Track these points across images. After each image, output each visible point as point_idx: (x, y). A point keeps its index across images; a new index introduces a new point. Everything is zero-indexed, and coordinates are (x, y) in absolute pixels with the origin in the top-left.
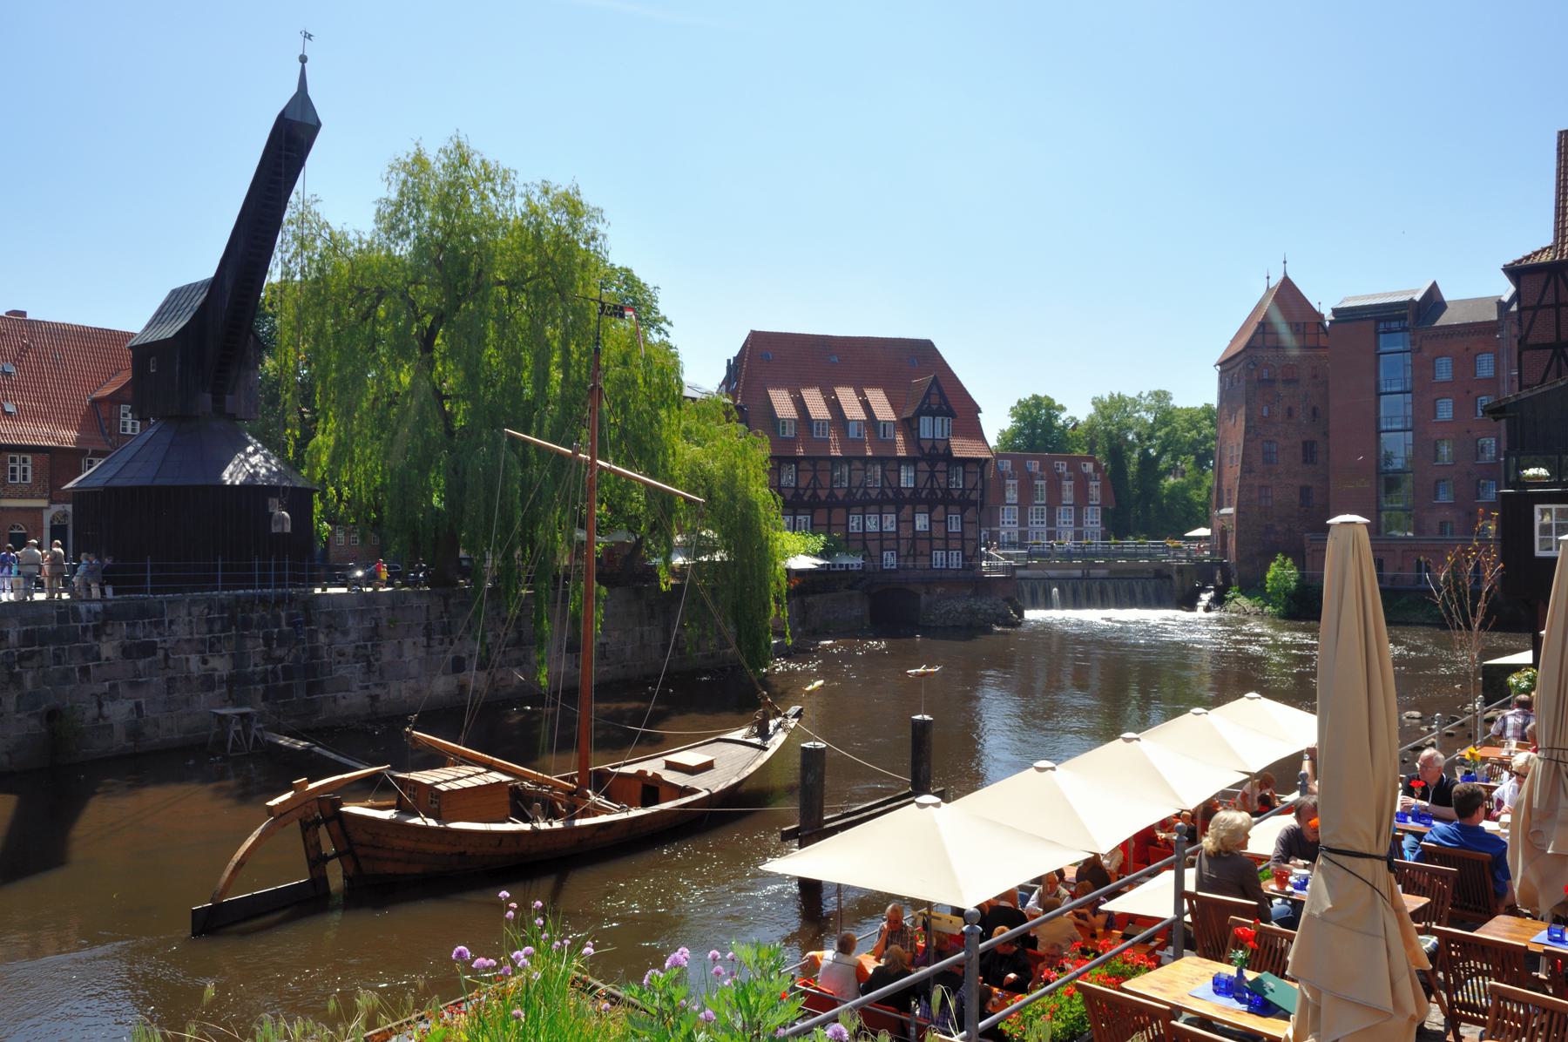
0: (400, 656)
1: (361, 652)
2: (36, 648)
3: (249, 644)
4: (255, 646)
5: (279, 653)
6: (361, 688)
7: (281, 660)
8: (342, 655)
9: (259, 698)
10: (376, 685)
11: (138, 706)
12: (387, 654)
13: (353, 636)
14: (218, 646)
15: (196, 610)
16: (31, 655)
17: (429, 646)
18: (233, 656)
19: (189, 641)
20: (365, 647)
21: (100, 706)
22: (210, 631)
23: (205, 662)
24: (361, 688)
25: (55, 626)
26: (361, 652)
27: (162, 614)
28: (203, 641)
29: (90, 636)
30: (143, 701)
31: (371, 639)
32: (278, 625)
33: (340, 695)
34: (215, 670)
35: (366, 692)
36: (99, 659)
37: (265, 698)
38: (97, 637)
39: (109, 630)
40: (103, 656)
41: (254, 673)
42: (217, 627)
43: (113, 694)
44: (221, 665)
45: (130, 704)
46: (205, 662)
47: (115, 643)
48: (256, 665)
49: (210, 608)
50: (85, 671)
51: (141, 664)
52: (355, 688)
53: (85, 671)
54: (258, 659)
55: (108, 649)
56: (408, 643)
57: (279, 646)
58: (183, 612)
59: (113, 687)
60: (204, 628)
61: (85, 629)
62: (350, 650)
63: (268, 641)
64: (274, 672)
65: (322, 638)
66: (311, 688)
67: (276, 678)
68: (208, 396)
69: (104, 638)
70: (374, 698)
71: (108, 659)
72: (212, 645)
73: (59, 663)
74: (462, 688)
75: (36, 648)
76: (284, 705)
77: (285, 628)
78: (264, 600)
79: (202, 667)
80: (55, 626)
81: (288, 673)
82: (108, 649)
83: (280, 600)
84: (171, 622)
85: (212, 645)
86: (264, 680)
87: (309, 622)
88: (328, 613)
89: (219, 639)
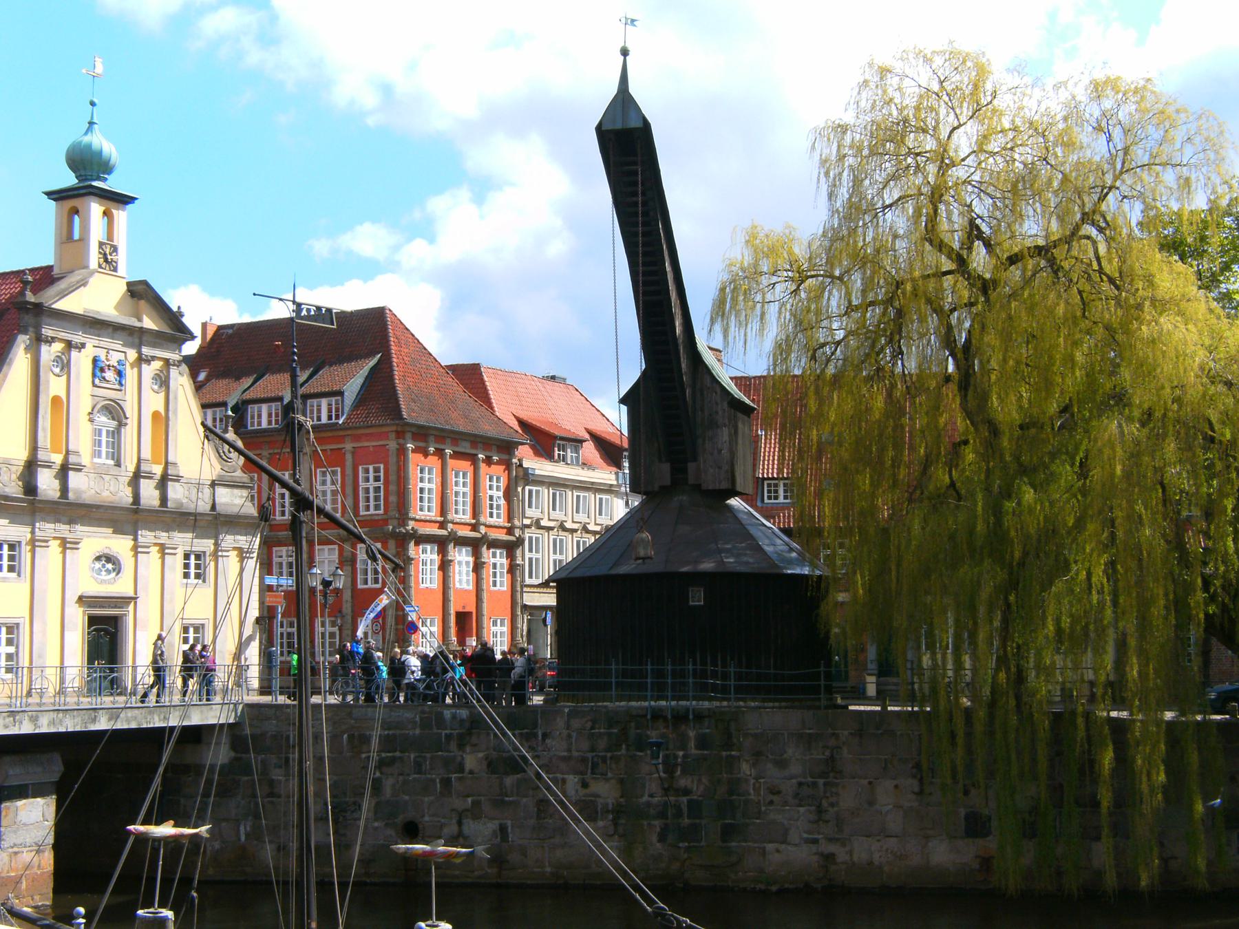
2: (398, 754)
4: (651, 773)
5: (683, 782)
6: (807, 841)
7: (686, 792)
8: (775, 791)
9: (654, 838)
10: (831, 840)
11: (503, 829)
12: (848, 797)
13: (795, 769)
15: (576, 723)
16: (393, 761)
17: (921, 792)
18: (621, 781)
19: (564, 759)
20: (815, 784)
21: (460, 823)
22: (593, 750)
24: (807, 841)
25: (417, 731)
27: (535, 726)
28: (584, 760)
29: (453, 746)
30: (509, 823)
31: (823, 775)
32: (683, 747)
33: (770, 847)
34: (599, 796)
35: (814, 848)
36: (461, 768)
37: (662, 838)
38: (461, 746)
39: (474, 740)
41: (648, 804)
42: (602, 744)
43: (475, 812)
44: (606, 791)
45: (493, 826)
46: (585, 785)
47: (481, 755)
48: (651, 793)
49: (594, 722)
50: (446, 782)
51: (509, 781)
52: (794, 836)
53: (446, 782)
54: (653, 786)
55: (471, 761)
57: (684, 772)
58: (560, 723)
59: (476, 804)
60: (585, 745)
61: (449, 737)
64: (678, 807)
65: (745, 768)
66: (728, 832)
67: (679, 814)
68: (666, 467)
69: (468, 749)
70: (829, 858)
71: (471, 772)
72: (594, 766)
73: (419, 772)
74: (986, 863)
75: (398, 754)
76: (688, 849)
77: (694, 751)
78: (657, 715)
79: (582, 792)
80: (417, 731)
81: (695, 808)
83: (680, 718)
84: (545, 736)
85: (594, 766)
86: (662, 815)
87: (728, 746)
89: (604, 760)
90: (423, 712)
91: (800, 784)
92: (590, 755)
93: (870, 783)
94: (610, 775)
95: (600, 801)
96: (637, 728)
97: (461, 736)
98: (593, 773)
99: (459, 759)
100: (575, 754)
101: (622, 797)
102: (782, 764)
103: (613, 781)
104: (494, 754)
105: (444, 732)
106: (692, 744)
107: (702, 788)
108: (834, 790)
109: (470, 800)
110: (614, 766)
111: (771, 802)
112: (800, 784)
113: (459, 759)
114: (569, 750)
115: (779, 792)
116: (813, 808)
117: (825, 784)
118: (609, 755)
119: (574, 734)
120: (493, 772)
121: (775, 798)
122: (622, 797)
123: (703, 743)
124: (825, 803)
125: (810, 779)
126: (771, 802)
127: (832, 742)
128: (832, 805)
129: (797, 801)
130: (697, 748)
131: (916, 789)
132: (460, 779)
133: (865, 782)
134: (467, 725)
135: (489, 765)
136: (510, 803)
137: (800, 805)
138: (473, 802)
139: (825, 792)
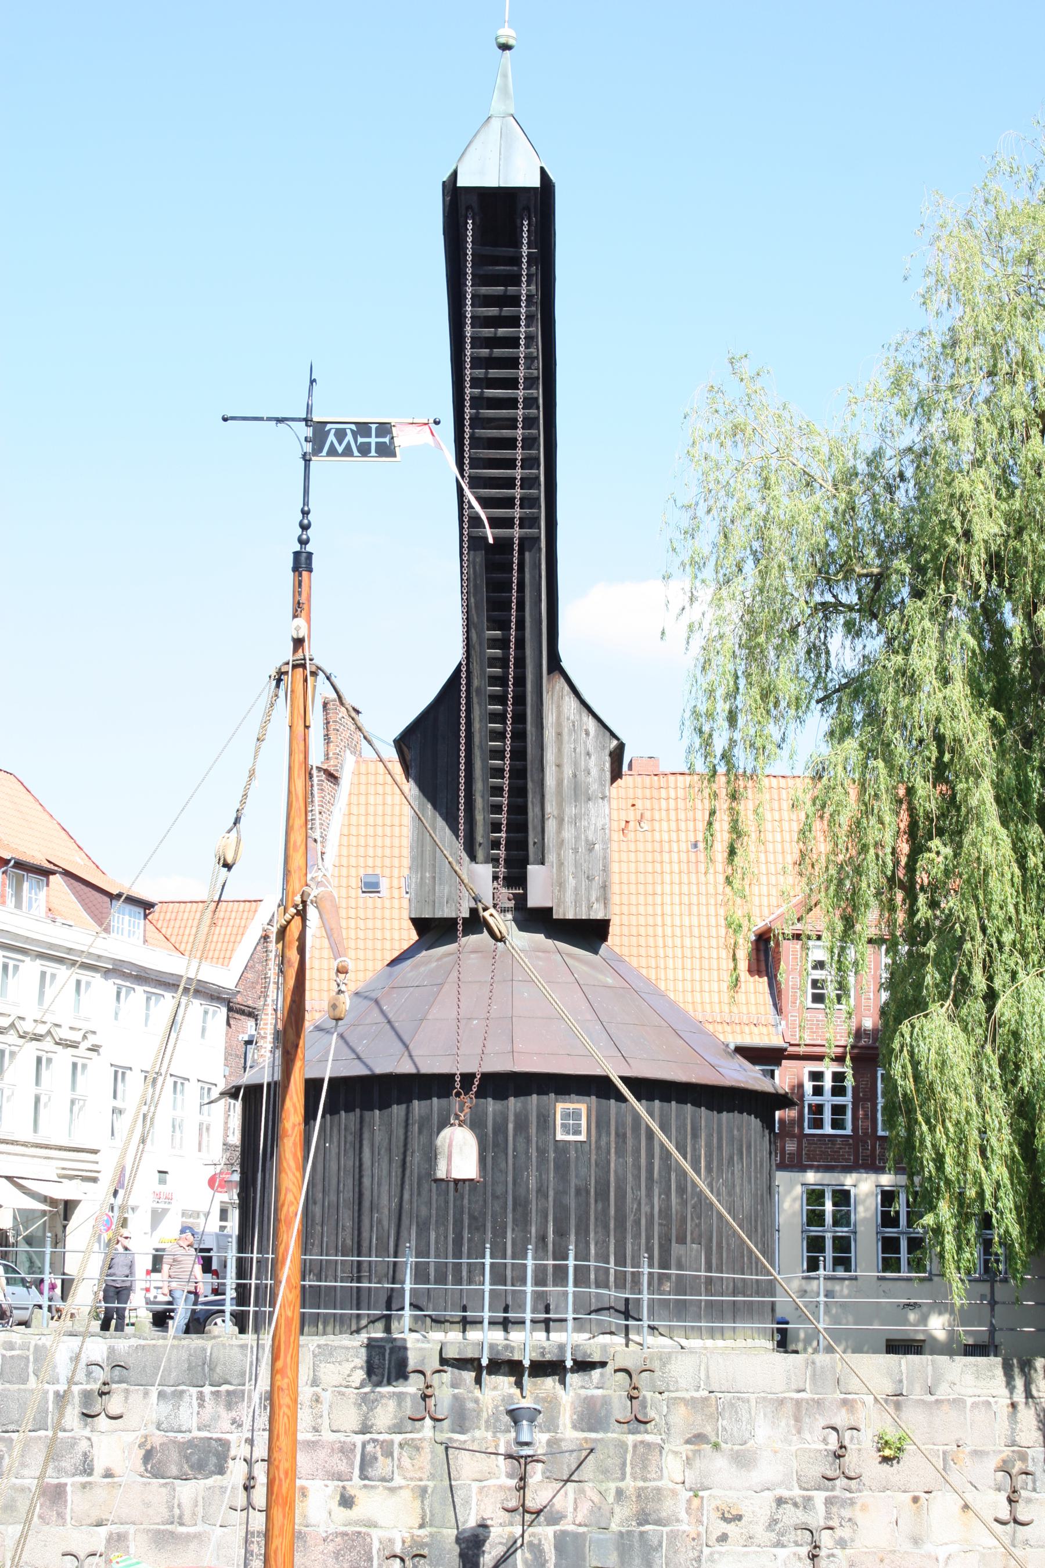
0: (916, 1541)
1: (791, 1516)
3: (467, 1465)
14: (382, 1466)
20: (809, 1499)
22: (365, 1429)
23: (347, 1501)
26: (791, 1516)
28: (345, 1450)
32: (552, 1426)
36: (86, 1468)
39: (114, 1404)
40: (99, 1469)
42: (385, 1415)
46: (347, 1501)
47: (132, 1438)
50: (56, 1494)
51: (188, 1491)
56: (944, 1506)
59: (118, 1540)
60: (350, 1417)
61: (61, 1399)
62: (758, 1509)
63: (520, 1461)
64: (537, 1549)
65: (672, 1468)
71: (108, 1474)
72: (366, 1462)
77: (570, 1435)
82: (114, 1447)
85: (366, 1462)
88: (692, 1403)
90: (10, 1346)
91: (780, 1501)
92: (359, 1439)
93: (916, 1500)
94: (399, 1480)
95: (376, 1534)
96: (454, 1386)
97: (87, 1396)
98: (363, 1476)
99: (84, 1445)
100: (327, 1436)
101: (422, 1526)
102: (743, 1460)
103: (406, 1494)
104: (157, 1438)
105: (52, 1389)
106: (566, 1418)
107: (585, 1507)
108: (846, 1513)
109: (103, 1531)
110: (406, 1462)
111: (723, 1538)
112: (780, 1501)
113: (84, 1445)
114: (316, 1430)
115: (739, 1518)
116: (804, 1551)
117: (829, 1502)
118: (398, 1438)
119: (326, 1397)
120: (157, 1473)
121: (731, 1529)
122: (422, 1526)
123: (591, 1417)
124: (826, 1539)
125: (797, 1493)
126: (723, 1538)
127: (841, 1419)
128: (842, 1543)
129: (773, 1536)
130: (575, 1427)
131: (1005, 1514)
132: (84, 1486)
133: (908, 1496)
134: (100, 1375)
135: (148, 1456)
136: (188, 1538)
137: (779, 1544)
138: (109, 1539)
139: (828, 1516)
